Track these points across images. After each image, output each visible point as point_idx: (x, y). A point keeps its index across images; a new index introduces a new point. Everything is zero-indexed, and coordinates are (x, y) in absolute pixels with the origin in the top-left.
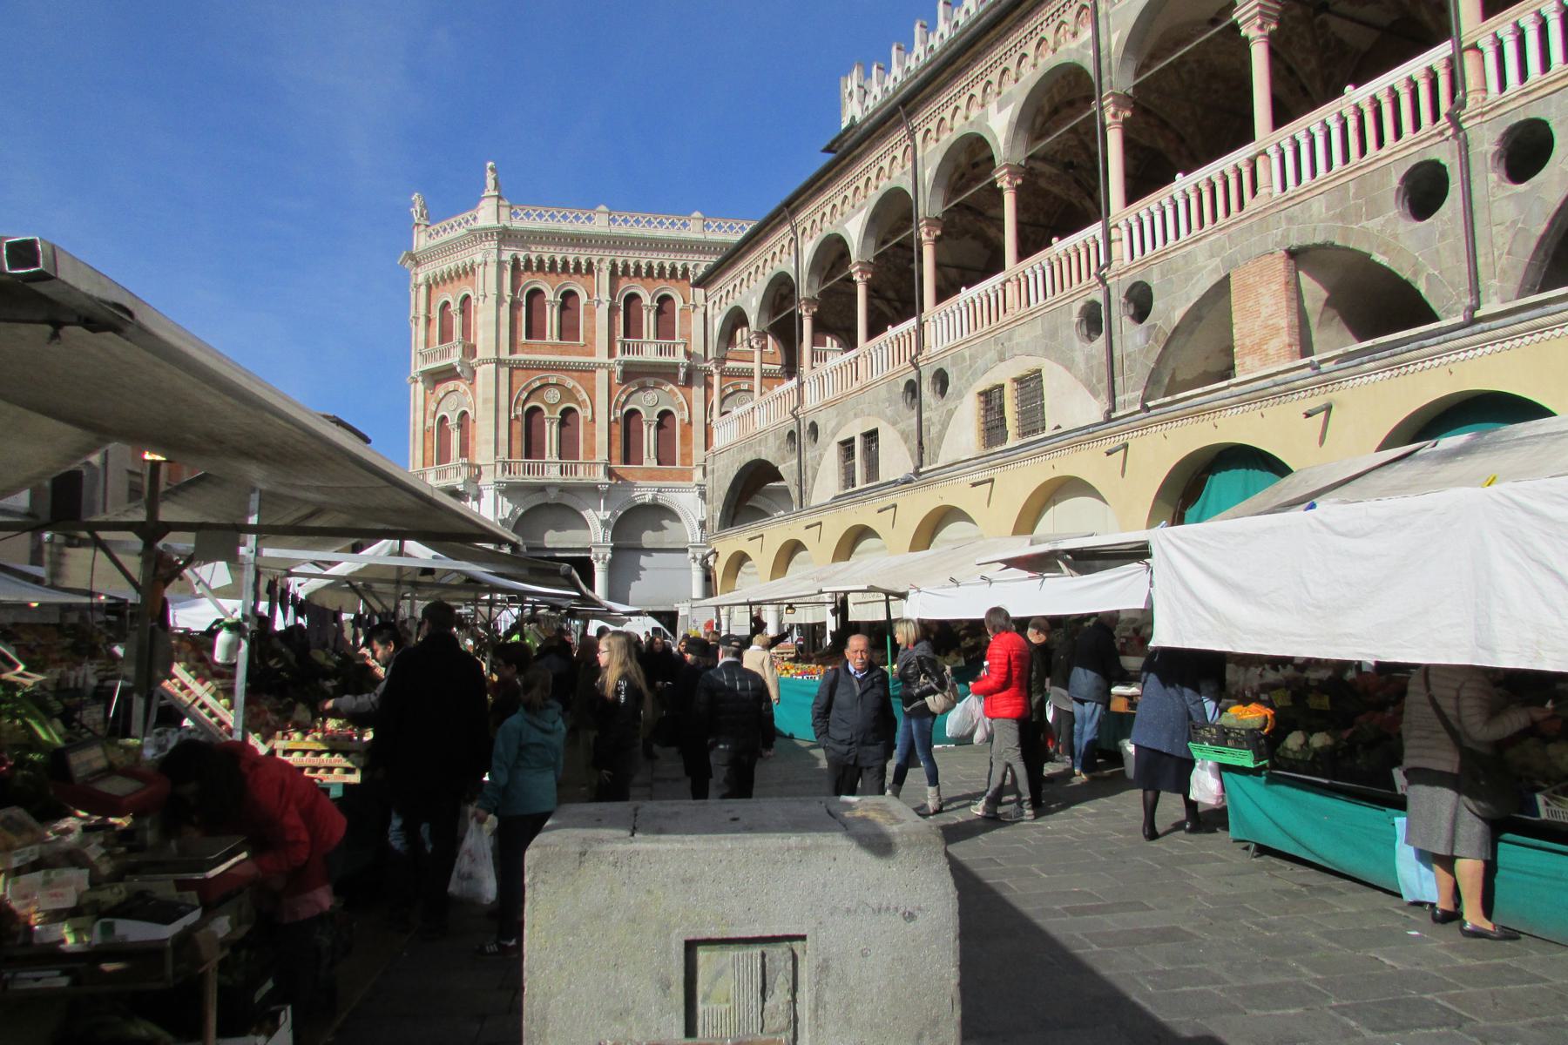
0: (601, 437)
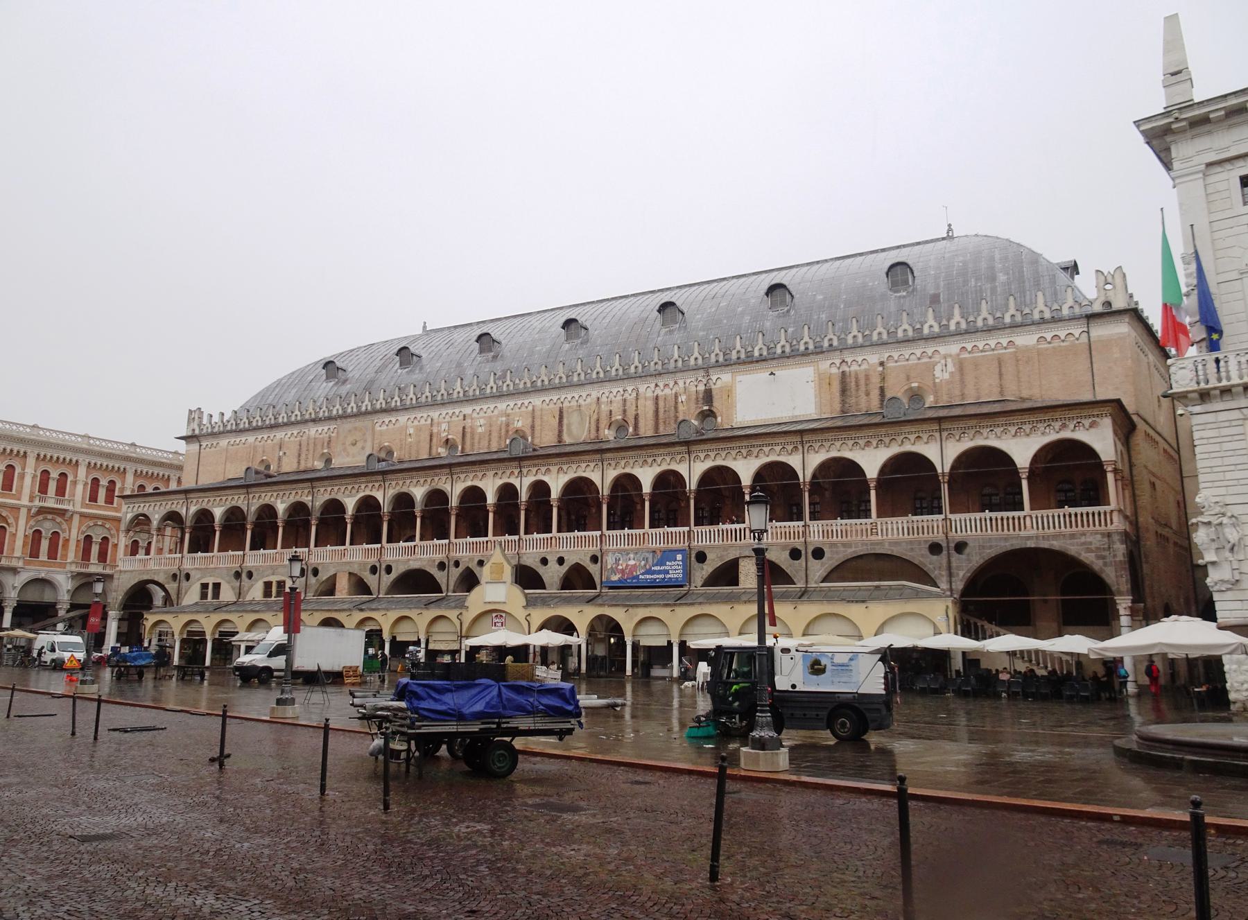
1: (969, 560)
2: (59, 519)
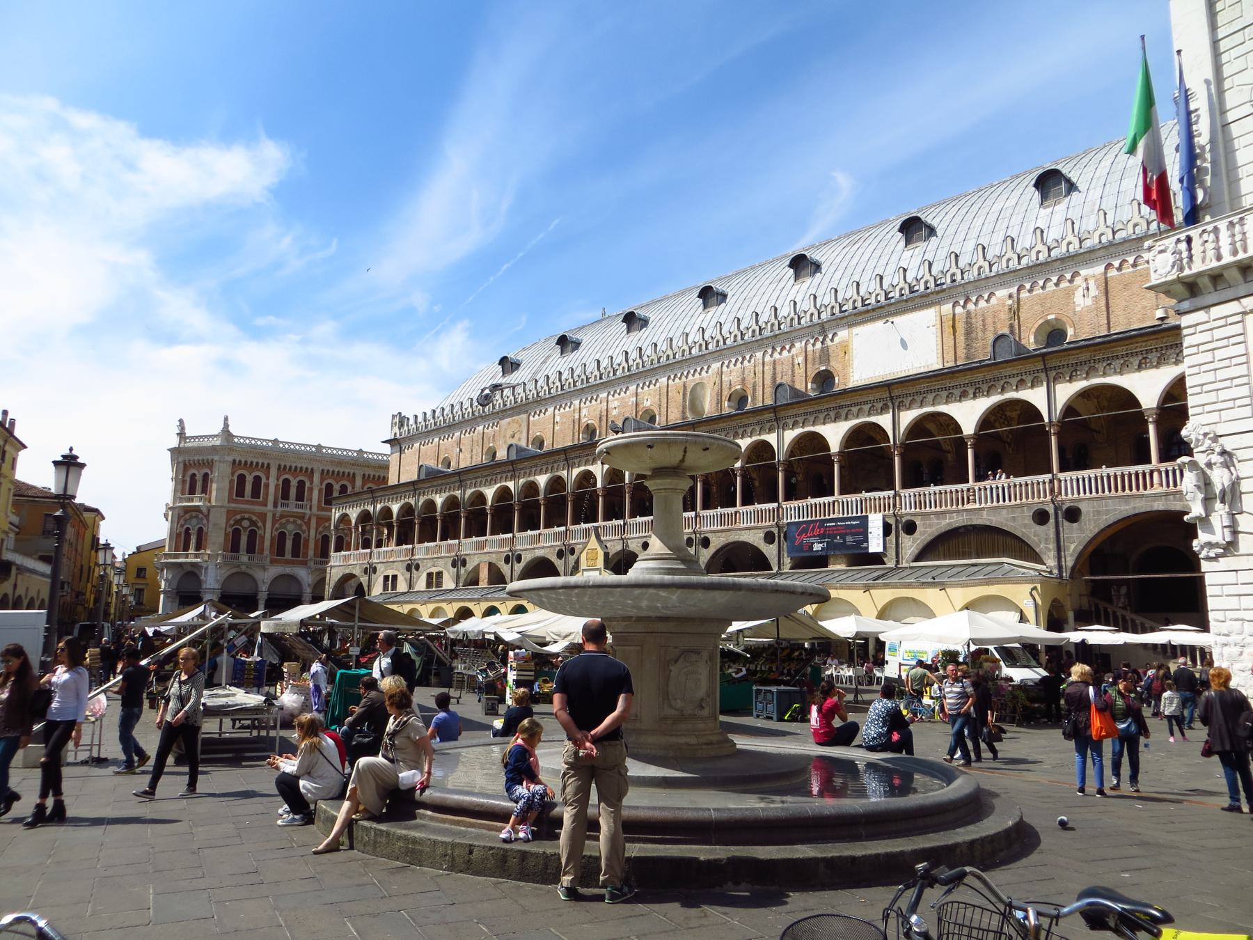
0: (267, 543)
1: (1081, 529)
2: (299, 522)
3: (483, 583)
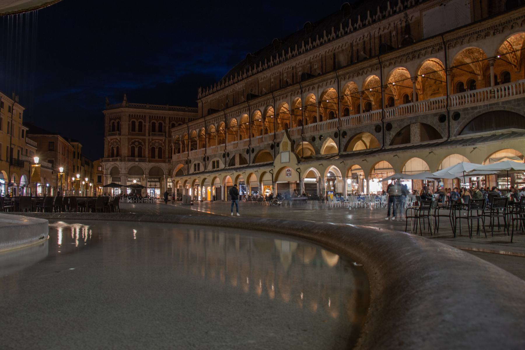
3: (237, 165)
